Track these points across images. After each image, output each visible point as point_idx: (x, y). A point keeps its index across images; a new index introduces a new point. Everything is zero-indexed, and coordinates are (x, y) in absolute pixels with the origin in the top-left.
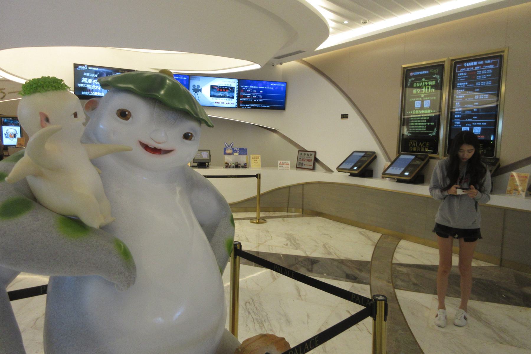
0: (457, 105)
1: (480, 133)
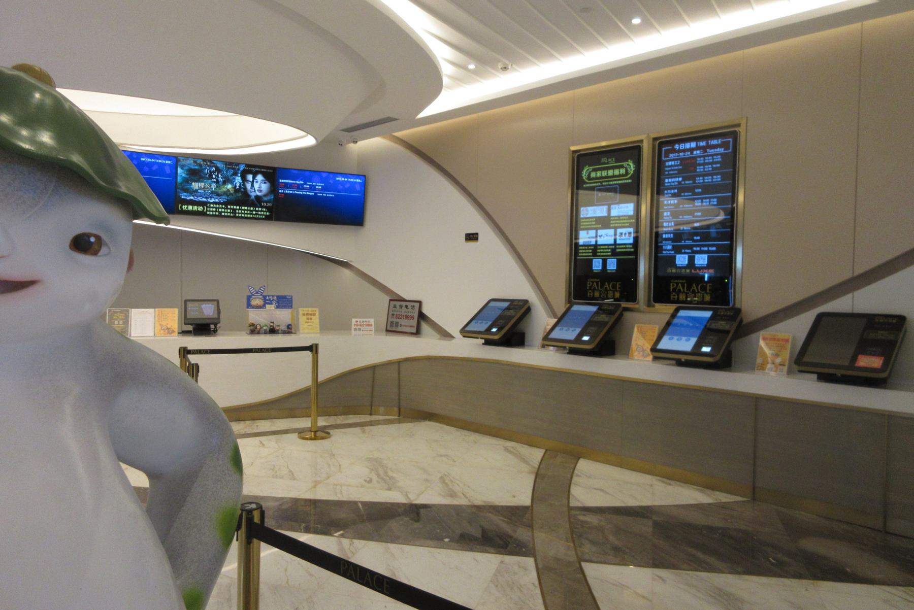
0: (666, 216)
1: (707, 265)
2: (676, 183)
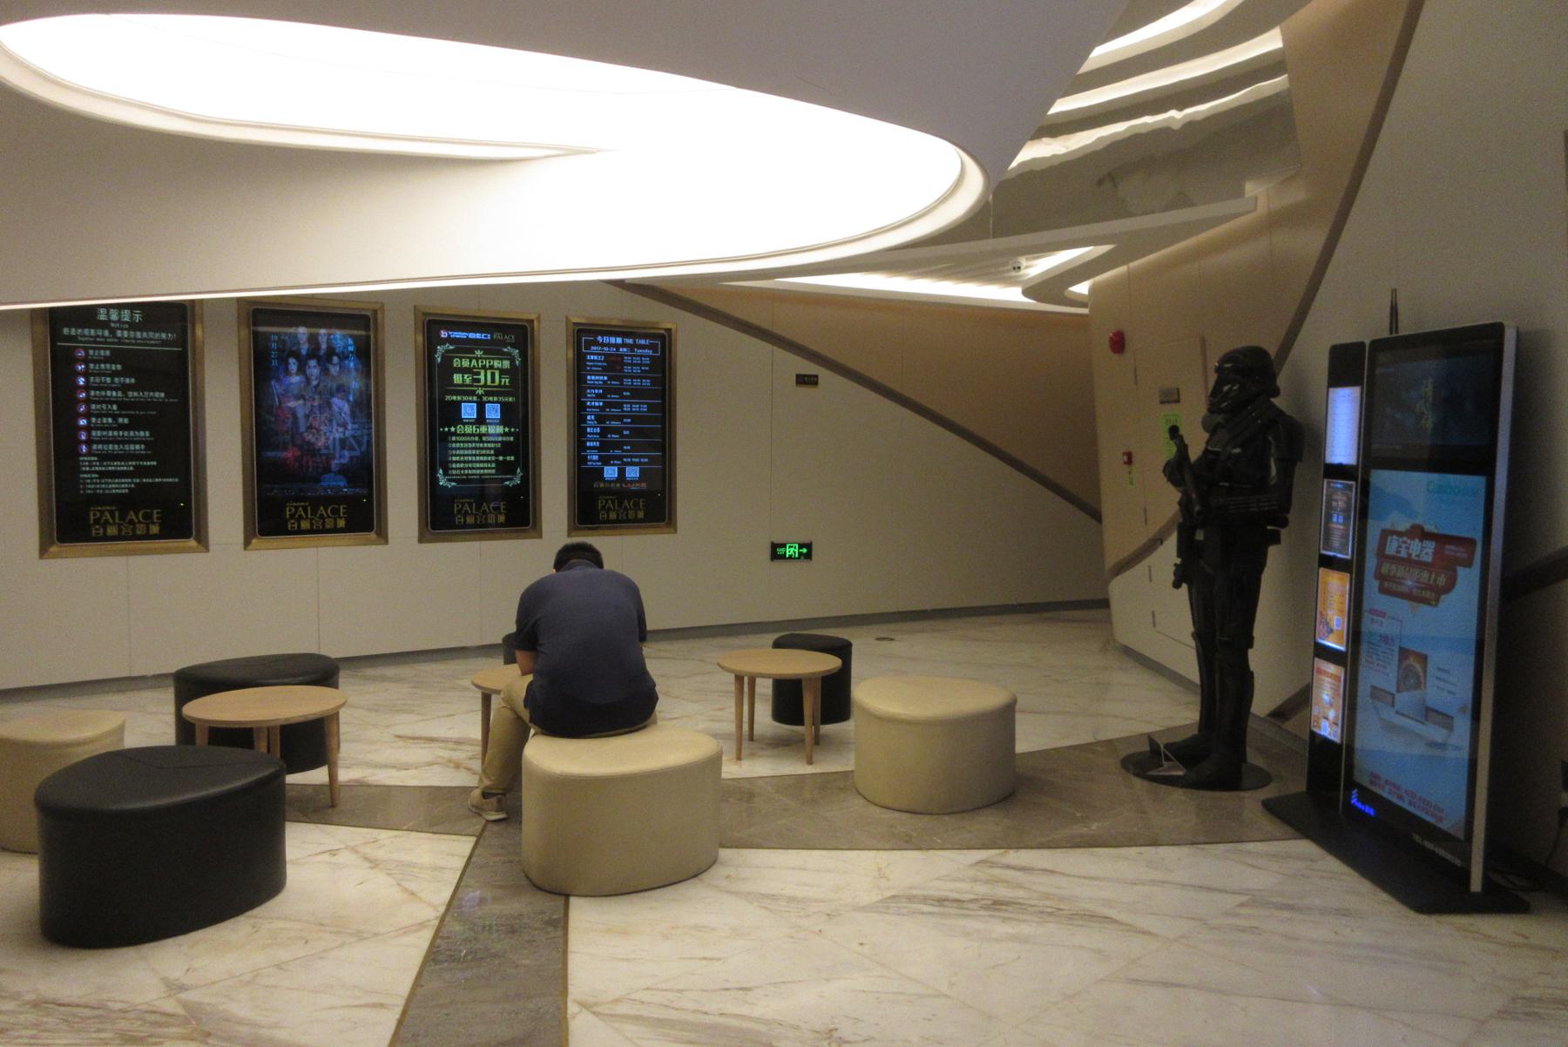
2: (601, 383)
